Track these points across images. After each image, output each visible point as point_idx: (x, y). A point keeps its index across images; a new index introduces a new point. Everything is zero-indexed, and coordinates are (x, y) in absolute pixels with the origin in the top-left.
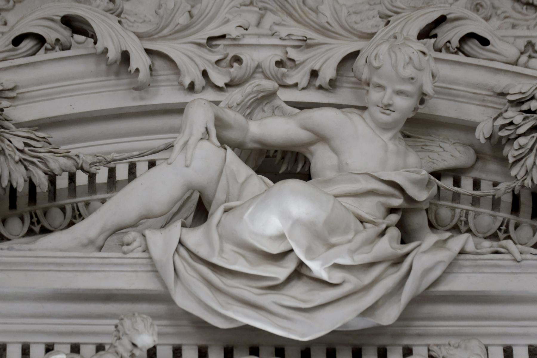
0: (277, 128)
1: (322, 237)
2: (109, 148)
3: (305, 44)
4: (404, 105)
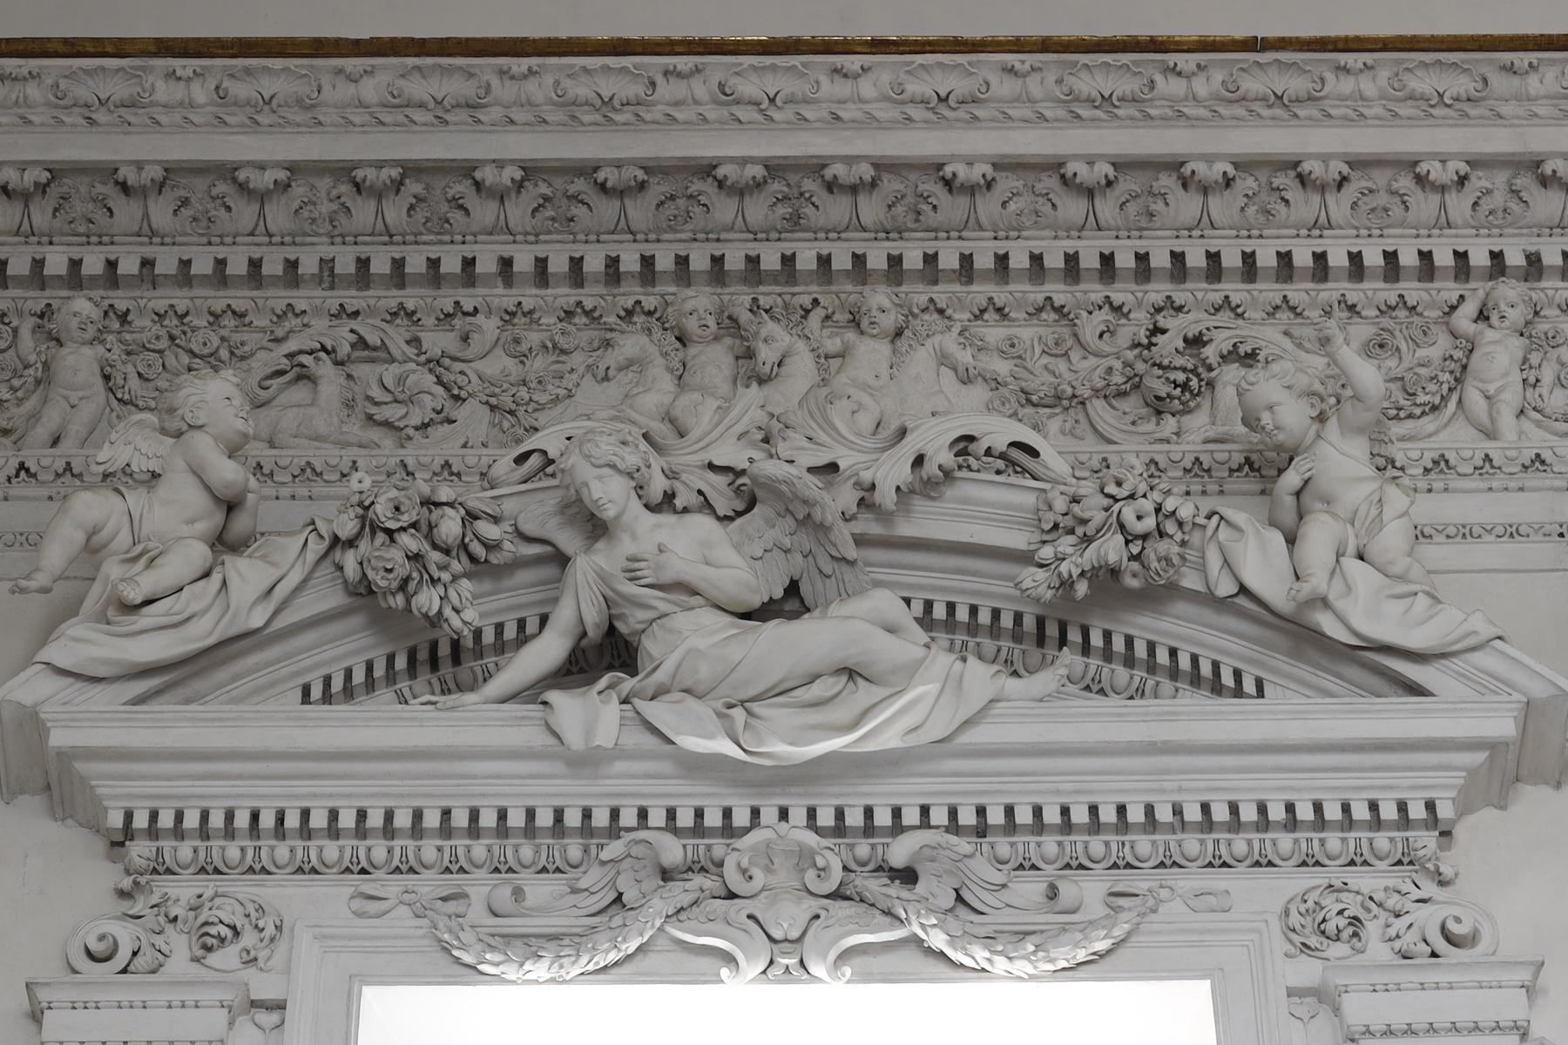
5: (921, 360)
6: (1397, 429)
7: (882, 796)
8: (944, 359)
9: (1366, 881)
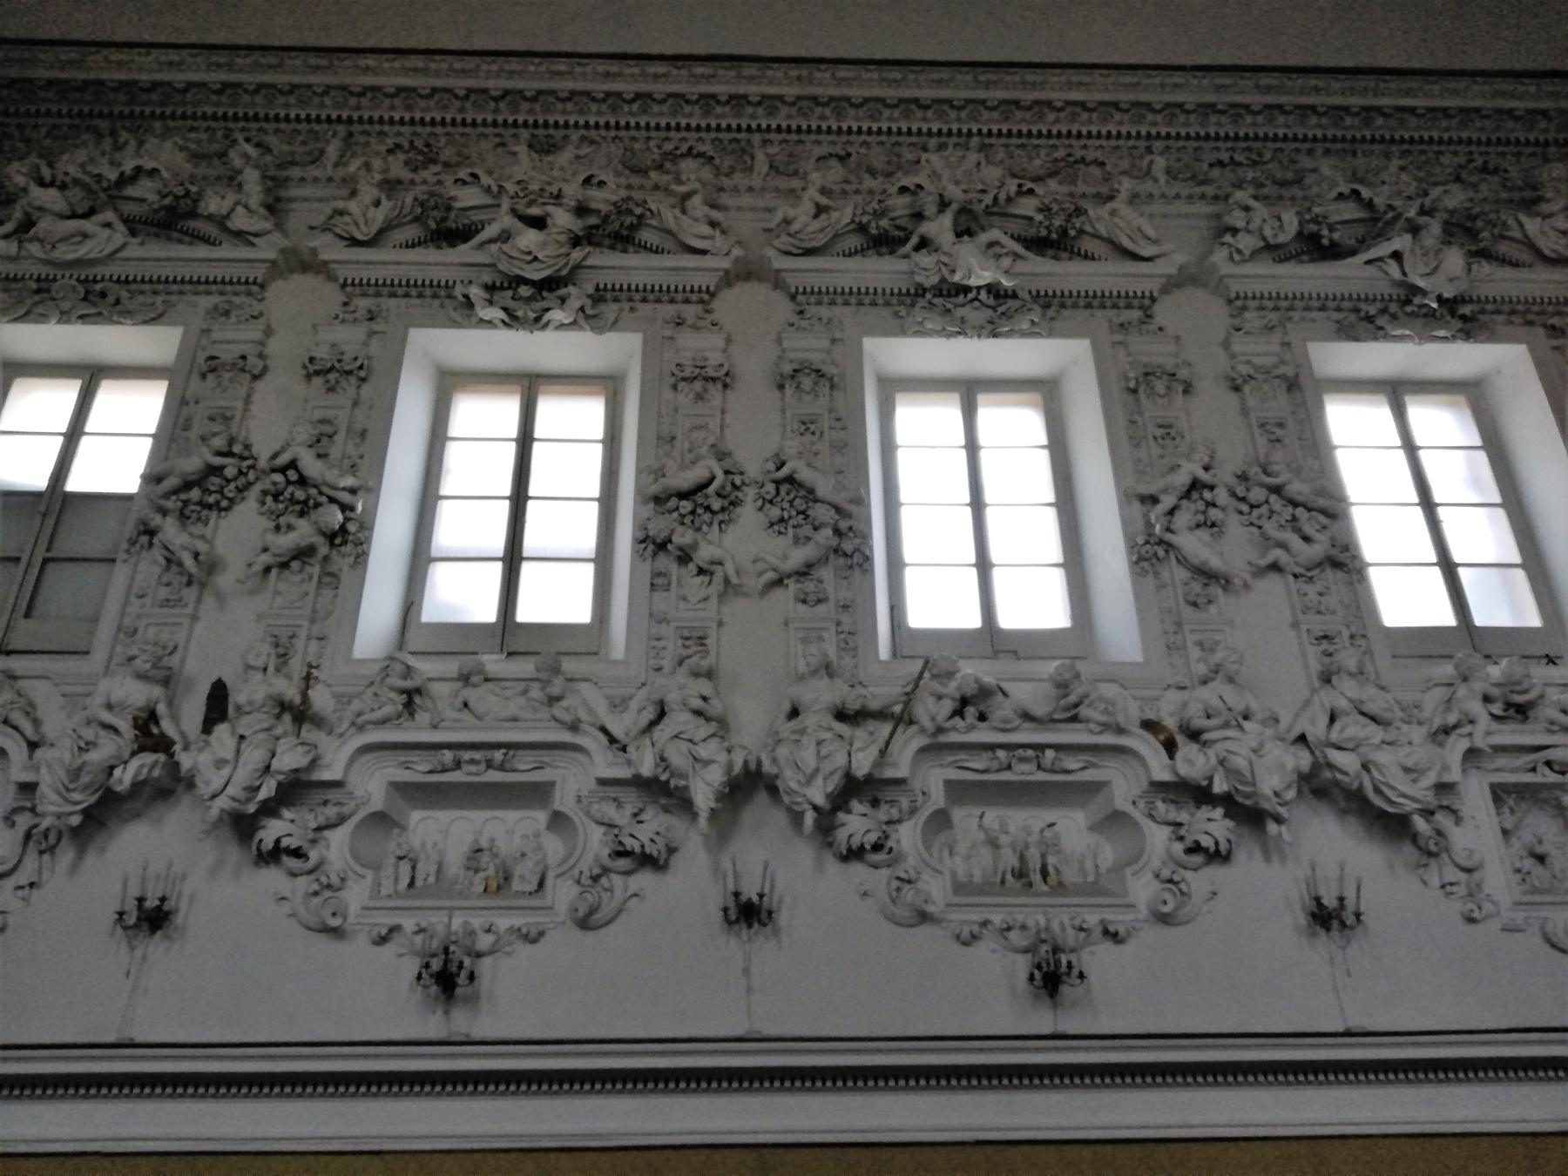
0: (535, 211)
1: (544, 245)
3: (549, 184)
4: (573, 203)
5: (168, 144)
6: (295, 172)
7: (99, 271)
8: (176, 143)
9: (237, 300)
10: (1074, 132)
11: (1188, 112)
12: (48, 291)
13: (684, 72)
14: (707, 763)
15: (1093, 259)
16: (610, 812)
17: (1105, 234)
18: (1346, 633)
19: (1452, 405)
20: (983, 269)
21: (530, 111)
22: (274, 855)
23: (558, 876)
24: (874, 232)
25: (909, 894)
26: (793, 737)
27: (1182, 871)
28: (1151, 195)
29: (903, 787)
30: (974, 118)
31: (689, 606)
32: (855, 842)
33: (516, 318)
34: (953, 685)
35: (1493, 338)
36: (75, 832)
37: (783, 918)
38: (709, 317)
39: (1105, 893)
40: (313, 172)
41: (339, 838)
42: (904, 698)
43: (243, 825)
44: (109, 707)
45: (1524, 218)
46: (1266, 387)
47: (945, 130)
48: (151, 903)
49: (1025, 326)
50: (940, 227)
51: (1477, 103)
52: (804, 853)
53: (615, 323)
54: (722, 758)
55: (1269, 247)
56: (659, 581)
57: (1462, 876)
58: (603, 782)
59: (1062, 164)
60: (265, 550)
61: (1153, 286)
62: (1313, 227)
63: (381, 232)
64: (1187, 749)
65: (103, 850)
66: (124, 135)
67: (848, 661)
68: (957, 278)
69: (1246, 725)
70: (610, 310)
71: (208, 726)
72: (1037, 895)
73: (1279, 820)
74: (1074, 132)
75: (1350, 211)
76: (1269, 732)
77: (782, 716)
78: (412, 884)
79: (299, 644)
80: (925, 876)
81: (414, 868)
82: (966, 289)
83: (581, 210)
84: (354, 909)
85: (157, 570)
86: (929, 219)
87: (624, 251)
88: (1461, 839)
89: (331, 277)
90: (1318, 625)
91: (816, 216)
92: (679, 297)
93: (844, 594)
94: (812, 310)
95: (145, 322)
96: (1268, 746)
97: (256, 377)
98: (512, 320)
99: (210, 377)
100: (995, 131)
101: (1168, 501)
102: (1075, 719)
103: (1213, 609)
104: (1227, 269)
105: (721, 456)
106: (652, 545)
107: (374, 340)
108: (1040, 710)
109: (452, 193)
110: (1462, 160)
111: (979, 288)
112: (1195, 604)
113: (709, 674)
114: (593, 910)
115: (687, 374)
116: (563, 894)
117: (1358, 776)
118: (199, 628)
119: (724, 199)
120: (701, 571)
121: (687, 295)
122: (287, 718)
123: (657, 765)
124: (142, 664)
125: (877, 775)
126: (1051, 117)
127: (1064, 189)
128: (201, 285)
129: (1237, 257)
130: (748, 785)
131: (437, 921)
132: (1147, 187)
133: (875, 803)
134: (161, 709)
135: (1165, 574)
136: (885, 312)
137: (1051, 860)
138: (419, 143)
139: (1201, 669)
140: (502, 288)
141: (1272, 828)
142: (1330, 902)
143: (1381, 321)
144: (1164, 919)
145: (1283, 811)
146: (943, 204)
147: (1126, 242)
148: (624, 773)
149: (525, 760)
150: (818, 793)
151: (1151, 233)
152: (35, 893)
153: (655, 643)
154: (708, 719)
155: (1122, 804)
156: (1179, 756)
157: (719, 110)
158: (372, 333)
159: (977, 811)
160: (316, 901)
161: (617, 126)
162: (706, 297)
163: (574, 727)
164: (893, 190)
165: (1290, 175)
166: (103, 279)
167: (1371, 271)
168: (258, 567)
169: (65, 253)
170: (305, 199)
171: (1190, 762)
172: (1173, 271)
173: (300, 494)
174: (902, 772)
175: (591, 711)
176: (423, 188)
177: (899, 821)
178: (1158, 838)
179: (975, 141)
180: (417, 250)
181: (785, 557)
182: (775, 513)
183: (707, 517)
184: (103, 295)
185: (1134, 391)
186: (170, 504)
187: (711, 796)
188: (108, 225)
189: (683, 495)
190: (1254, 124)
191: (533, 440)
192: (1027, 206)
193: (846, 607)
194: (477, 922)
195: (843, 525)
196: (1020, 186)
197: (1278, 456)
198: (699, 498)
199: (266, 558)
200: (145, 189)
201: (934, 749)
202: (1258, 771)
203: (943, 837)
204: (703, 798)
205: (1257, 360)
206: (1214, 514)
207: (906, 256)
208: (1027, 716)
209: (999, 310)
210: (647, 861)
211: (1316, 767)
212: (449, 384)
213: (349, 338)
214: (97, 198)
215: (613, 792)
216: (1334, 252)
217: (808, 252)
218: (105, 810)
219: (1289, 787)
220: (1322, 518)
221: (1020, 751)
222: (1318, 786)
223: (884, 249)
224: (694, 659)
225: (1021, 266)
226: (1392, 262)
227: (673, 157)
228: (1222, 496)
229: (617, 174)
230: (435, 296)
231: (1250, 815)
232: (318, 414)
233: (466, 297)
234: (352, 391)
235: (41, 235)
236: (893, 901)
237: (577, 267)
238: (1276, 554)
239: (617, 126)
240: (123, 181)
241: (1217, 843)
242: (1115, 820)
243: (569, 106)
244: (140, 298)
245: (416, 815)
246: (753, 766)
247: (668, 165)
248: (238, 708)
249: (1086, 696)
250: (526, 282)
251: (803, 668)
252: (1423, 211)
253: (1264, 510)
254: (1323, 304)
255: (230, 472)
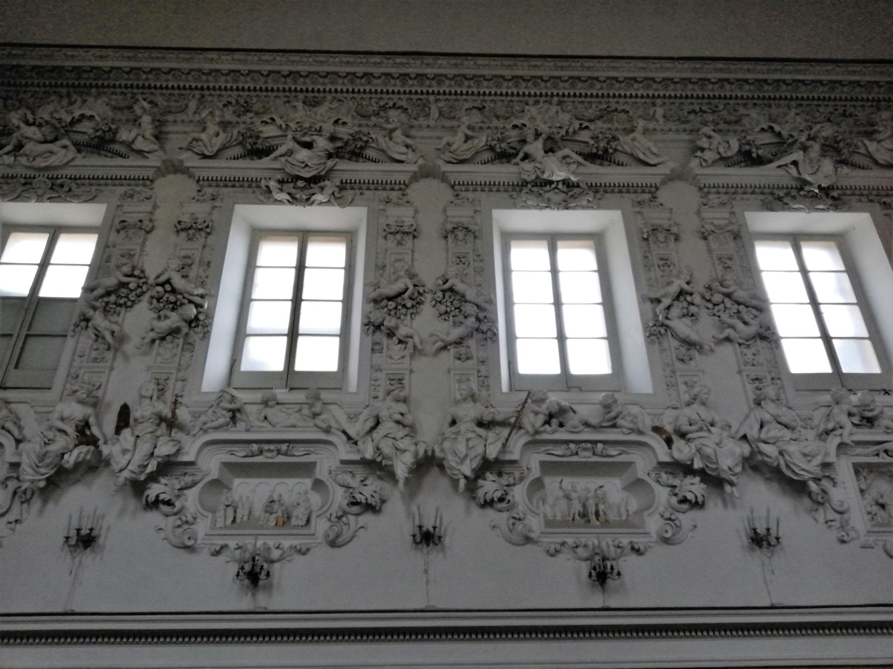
0: (307, 139)
1: (310, 158)
2: (276, 142)
4: (328, 135)
5: (100, 101)
6: (170, 118)
7: (60, 172)
10: (611, 94)
11: (676, 83)
12: (31, 184)
13: (391, 61)
14: (405, 451)
15: (622, 165)
16: (348, 479)
17: (629, 151)
18: (769, 378)
19: (828, 247)
20: (560, 171)
21: (304, 83)
22: (155, 504)
23: (318, 516)
24: (499, 150)
25: (519, 527)
26: (453, 436)
27: (677, 514)
28: (655, 130)
29: (515, 465)
30: (555, 86)
31: (393, 361)
32: (488, 498)
33: (296, 199)
34: (544, 406)
35: (850, 209)
36: (42, 491)
37: (447, 541)
38: (405, 199)
39: (634, 527)
40: (181, 117)
41: (192, 495)
42: (516, 414)
43: (137, 487)
44: (62, 419)
45: (866, 142)
46: (722, 237)
47: (538, 93)
48: (84, 532)
49: (584, 203)
50: (536, 148)
51: (840, 78)
52: (459, 503)
53: (351, 202)
54: (412, 448)
55: (722, 159)
56: (377, 347)
57: (838, 516)
58: (343, 462)
59: (605, 112)
60: (152, 330)
61: (657, 180)
62: (748, 148)
63: (219, 150)
64: (678, 443)
65: (57, 502)
66: (75, 96)
67: (484, 393)
68: (545, 176)
69: (713, 429)
70: (349, 194)
71: (118, 430)
72: (593, 527)
73: (732, 484)
74: (611, 94)
75: (768, 138)
76: (725, 433)
77: (446, 425)
78: (234, 521)
79: (171, 383)
80: (528, 517)
81: (235, 512)
82: (551, 182)
83: (333, 138)
84: (201, 535)
85: (91, 342)
86: (530, 143)
87: (357, 161)
88: (836, 495)
89: (191, 176)
90: (753, 372)
91: (466, 142)
92: (388, 187)
93: (482, 354)
94: (463, 194)
95: (85, 202)
96: (725, 441)
97: (148, 232)
98: (294, 200)
99: (122, 233)
100: (566, 94)
101: (666, 302)
102: (614, 426)
103: (692, 363)
104: (698, 171)
105: (412, 276)
106: (372, 326)
107: (215, 212)
108: (594, 421)
109: (260, 129)
110: (830, 109)
111: (558, 182)
112: (682, 360)
113: (405, 400)
114: (338, 536)
115: (392, 230)
116: (321, 526)
117: (777, 459)
118: (114, 373)
119: (413, 132)
120: (400, 342)
121: (390, 186)
122: (164, 425)
123: (375, 452)
124: (82, 395)
125: (501, 458)
126: (598, 86)
127: (606, 126)
128: (116, 180)
129: (704, 164)
130: (427, 464)
131: (249, 542)
132: (651, 126)
133: (500, 474)
134: (92, 420)
135: (665, 344)
136: (505, 195)
137: (601, 507)
138: (242, 101)
139: (686, 398)
140: (287, 182)
141: (728, 488)
142: (761, 531)
143: (786, 200)
144: (666, 541)
145: (733, 478)
146: (538, 135)
147: (641, 156)
148: (356, 457)
149: (300, 450)
150: (467, 469)
151: (655, 150)
152: (18, 527)
153: (374, 383)
154: (404, 426)
155: (641, 475)
156: (674, 447)
157: (410, 82)
158: (214, 207)
159: (559, 480)
160: (180, 530)
161: (353, 92)
162: (403, 187)
163: (327, 431)
164: (509, 127)
165: (733, 118)
166: (62, 177)
167: (781, 172)
168: (147, 340)
169: (40, 163)
170: (177, 133)
171: (680, 450)
172: (668, 172)
173: (172, 298)
174: (515, 456)
175: (337, 421)
176: (243, 126)
177: (514, 485)
178: (662, 494)
179: (556, 99)
180: (240, 160)
181: (448, 334)
182: (443, 308)
183: (404, 311)
184: (62, 186)
185: (647, 240)
186: (97, 304)
187: (406, 470)
188: (65, 147)
189: (390, 299)
190: (713, 90)
191: (305, 267)
192: (585, 136)
193: (483, 362)
194: (271, 543)
195: (481, 315)
196: (581, 124)
197: (729, 277)
198: (399, 300)
199: (152, 335)
200: (86, 127)
201: (534, 443)
202: (719, 456)
203: (539, 494)
204: (401, 471)
205: (716, 222)
206: (693, 309)
207: (517, 164)
208: (587, 424)
209: (570, 194)
210: (369, 508)
211: (752, 453)
212: (258, 235)
213: (201, 210)
214: (58, 132)
215: (351, 468)
216: (760, 161)
217: (462, 162)
218: (58, 479)
219: (737, 465)
220: (754, 311)
221: (583, 445)
222: (754, 464)
223: (504, 160)
224: (396, 392)
225: (582, 170)
226: (793, 167)
227: (384, 108)
228: (697, 299)
229: (353, 118)
230: (250, 186)
231: (715, 481)
232: (183, 253)
233: (267, 187)
234: (202, 240)
235: (28, 152)
236: (511, 531)
237: (331, 170)
238: (728, 332)
239: (353, 92)
240: (73, 122)
241: (696, 497)
242: (637, 484)
243: (326, 80)
244: (83, 188)
245: (237, 481)
246: (430, 453)
247: (382, 113)
248: (136, 420)
249: (621, 412)
250: (302, 178)
251: (458, 397)
252: (810, 138)
253: (721, 307)
254: (754, 190)
255: (132, 286)
